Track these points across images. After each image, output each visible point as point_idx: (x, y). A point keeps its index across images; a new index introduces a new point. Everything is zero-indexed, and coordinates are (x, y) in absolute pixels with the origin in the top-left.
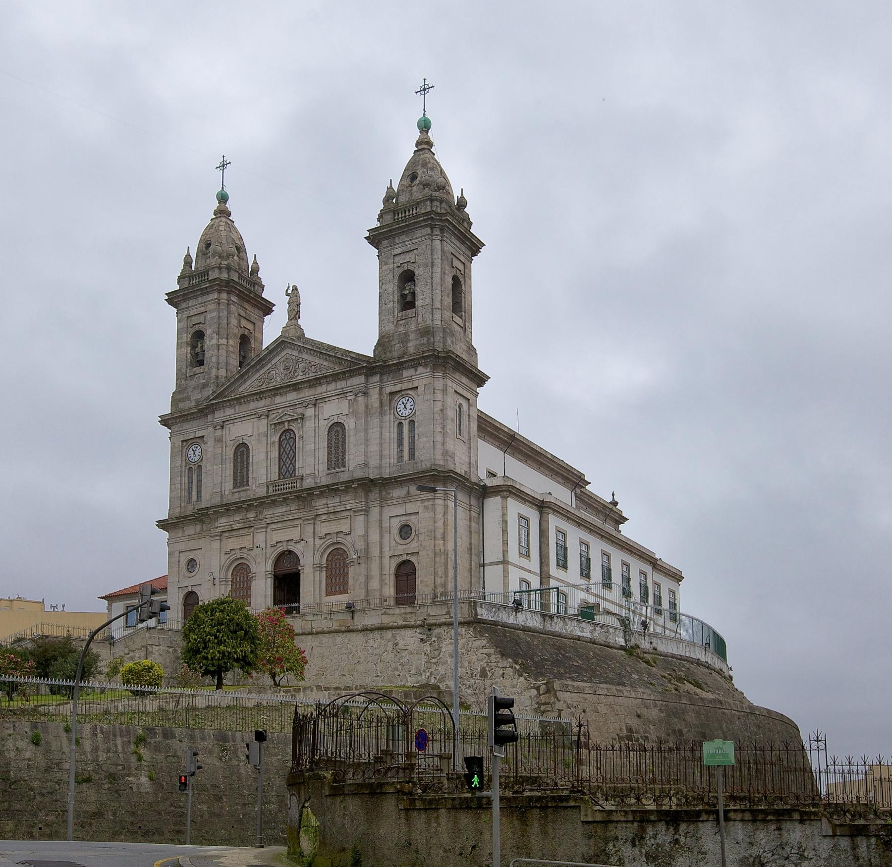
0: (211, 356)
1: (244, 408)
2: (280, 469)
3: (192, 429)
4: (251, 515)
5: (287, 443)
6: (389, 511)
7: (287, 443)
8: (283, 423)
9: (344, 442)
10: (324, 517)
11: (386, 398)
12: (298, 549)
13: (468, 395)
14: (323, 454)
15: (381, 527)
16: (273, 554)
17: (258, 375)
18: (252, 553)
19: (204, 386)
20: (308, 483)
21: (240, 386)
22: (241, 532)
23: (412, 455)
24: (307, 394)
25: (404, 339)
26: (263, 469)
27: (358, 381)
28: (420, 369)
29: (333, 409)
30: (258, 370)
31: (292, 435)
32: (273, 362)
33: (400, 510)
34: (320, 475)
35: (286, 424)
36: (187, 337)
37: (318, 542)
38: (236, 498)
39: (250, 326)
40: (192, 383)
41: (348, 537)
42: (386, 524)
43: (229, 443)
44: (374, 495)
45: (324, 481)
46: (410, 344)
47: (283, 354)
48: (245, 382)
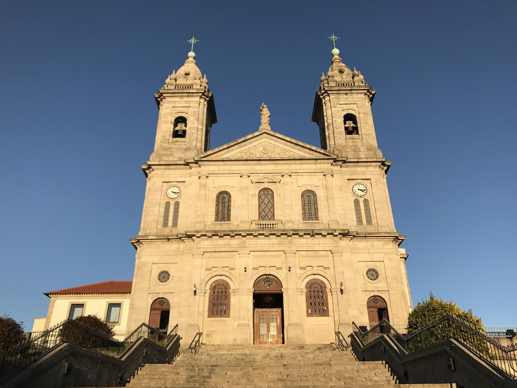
1: (226, 167)
2: (259, 214)
4: (236, 241)
5: (266, 197)
7: (266, 197)
9: (316, 203)
12: (281, 275)
17: (240, 150)
21: (226, 153)
22: (223, 254)
23: (369, 222)
25: (356, 150)
26: (245, 211)
27: (326, 166)
28: (370, 169)
29: (306, 182)
30: (241, 147)
31: (270, 192)
32: (254, 144)
33: (367, 257)
43: (212, 189)
44: (345, 242)
46: (361, 153)
48: (229, 152)
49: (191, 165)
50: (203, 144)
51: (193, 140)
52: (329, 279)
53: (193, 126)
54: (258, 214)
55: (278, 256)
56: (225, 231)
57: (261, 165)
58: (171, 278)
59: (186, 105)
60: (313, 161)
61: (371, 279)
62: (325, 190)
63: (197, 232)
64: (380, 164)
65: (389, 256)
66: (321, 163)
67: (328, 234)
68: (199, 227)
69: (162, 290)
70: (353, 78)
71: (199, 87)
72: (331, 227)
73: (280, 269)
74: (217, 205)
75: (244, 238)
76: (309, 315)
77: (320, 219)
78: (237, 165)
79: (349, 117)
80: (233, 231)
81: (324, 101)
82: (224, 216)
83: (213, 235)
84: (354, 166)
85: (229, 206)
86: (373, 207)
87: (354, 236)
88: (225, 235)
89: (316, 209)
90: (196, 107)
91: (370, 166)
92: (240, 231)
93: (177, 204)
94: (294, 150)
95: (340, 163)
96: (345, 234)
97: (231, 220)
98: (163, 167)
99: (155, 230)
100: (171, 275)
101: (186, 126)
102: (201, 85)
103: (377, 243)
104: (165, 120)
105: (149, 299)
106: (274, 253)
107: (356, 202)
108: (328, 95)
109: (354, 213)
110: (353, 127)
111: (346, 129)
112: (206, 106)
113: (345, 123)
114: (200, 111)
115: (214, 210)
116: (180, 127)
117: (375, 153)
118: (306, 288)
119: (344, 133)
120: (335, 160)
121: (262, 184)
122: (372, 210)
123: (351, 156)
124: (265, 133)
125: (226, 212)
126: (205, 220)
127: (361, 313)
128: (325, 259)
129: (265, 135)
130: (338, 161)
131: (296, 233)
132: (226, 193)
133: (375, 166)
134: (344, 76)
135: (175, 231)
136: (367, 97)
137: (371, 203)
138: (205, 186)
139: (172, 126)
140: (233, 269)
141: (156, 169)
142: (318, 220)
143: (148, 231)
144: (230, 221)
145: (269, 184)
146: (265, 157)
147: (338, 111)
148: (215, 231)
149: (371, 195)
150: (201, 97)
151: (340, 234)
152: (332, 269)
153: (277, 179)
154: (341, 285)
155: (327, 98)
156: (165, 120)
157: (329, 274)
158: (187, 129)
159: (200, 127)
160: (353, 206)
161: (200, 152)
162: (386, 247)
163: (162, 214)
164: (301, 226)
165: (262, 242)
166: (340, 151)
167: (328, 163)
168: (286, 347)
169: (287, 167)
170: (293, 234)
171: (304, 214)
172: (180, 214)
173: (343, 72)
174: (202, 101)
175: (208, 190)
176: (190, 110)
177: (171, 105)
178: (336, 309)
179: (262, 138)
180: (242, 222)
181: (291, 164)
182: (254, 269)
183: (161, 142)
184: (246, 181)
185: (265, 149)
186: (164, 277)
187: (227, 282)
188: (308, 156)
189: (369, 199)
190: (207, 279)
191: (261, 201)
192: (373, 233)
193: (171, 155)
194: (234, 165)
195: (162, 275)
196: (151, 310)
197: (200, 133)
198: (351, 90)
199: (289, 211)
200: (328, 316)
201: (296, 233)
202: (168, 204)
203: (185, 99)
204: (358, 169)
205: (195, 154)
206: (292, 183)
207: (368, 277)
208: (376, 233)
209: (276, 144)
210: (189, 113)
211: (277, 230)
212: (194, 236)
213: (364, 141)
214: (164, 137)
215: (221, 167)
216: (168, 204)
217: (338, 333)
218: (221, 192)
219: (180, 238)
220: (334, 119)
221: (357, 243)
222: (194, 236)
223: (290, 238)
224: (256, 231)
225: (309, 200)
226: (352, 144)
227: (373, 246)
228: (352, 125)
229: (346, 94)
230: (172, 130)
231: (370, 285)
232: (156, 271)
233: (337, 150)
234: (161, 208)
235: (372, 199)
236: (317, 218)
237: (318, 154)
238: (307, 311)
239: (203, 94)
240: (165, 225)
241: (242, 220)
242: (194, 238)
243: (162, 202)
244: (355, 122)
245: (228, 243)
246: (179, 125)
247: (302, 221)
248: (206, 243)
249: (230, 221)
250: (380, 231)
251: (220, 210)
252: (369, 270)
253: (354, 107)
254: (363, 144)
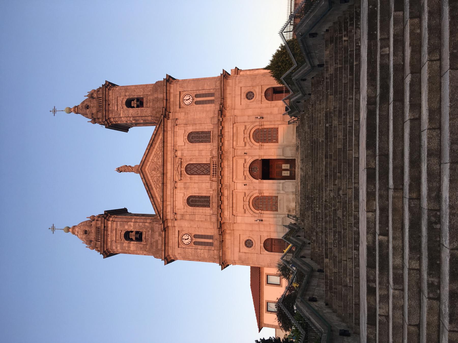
1: (169, 199)
4: (226, 193)
6: (238, 106)
9: (198, 133)
10: (235, 143)
12: (250, 160)
14: (201, 146)
17: (154, 189)
20: (215, 153)
22: (234, 201)
23: (212, 95)
25: (157, 100)
26: (202, 186)
27: (169, 124)
28: (172, 91)
30: (152, 188)
31: (189, 166)
32: (150, 178)
33: (238, 99)
34: (212, 147)
35: (182, 169)
38: (215, 205)
43: (185, 210)
44: (228, 113)
46: (159, 97)
47: (147, 172)
48: (156, 197)
49: (166, 226)
50: (147, 218)
51: (145, 225)
52: (252, 126)
53: (132, 226)
54: (205, 176)
55: (237, 161)
56: (218, 200)
57: (167, 173)
58: (250, 238)
59: (114, 232)
60: (165, 133)
61: (253, 97)
62: (188, 125)
63: (218, 220)
64: (168, 84)
65: (237, 83)
66: (167, 127)
67: (221, 125)
68: (214, 219)
69: (258, 245)
70: (94, 98)
71: (99, 223)
72: (216, 123)
73: (245, 160)
74: (198, 206)
75: (223, 186)
76: (277, 142)
77: (210, 130)
78: (166, 191)
79: (129, 104)
80: (218, 194)
81: (114, 123)
82: (206, 201)
83: (220, 208)
84: (169, 103)
85: (199, 197)
86: (201, 91)
87: (223, 106)
88: (220, 200)
89: (202, 132)
90: (117, 224)
91: (170, 90)
92: (218, 189)
93: (195, 236)
94: (156, 147)
95: (167, 113)
96: (222, 112)
97: (209, 195)
98: (167, 248)
99: (215, 252)
100: (248, 239)
101: (132, 232)
103: (228, 90)
104: (127, 248)
105: (264, 253)
106: (234, 164)
107: (197, 103)
108: (109, 119)
109: (205, 105)
110: (137, 101)
111: (138, 106)
112: (116, 216)
113: (133, 107)
114: (120, 220)
115: (202, 208)
116: (133, 236)
117: (159, 86)
118: (258, 143)
119: (142, 108)
120: (165, 116)
121: (182, 172)
122: (204, 92)
123: (161, 105)
124: (141, 169)
125: (203, 199)
126: (209, 214)
127: (276, 106)
128: (239, 128)
129: (143, 169)
130: (165, 114)
131: (220, 148)
132: (188, 199)
133: (170, 87)
134: (92, 105)
135: (217, 236)
136: (112, 89)
137: (198, 93)
138: (183, 215)
139: (132, 242)
140: (245, 194)
141: (168, 252)
142: (210, 132)
143: (216, 257)
144: (210, 197)
145: (182, 167)
146: (161, 169)
147: (124, 112)
148: (218, 207)
149: (192, 92)
150: (108, 220)
151: (221, 117)
152: (246, 124)
153: (178, 161)
154: (257, 118)
155: (112, 120)
156: (127, 248)
157: (249, 126)
158: (135, 230)
159: (133, 220)
160: (200, 105)
161: (155, 220)
162: (231, 85)
163: (203, 247)
164: (215, 144)
165: (226, 172)
166: (157, 112)
167: (167, 122)
168: (297, 157)
169: (169, 153)
170: (221, 150)
171: (206, 142)
172: (203, 234)
173: (88, 106)
174: (111, 219)
175: (186, 213)
177: (114, 244)
178: (273, 123)
179: (145, 171)
180: (211, 187)
181: (167, 150)
182: (245, 179)
183: (146, 251)
184: (179, 185)
185: (154, 170)
186: (249, 243)
187: (254, 198)
188: (161, 137)
189: (195, 94)
190: (252, 213)
191: (195, 173)
192: (221, 93)
193: (157, 242)
194: (166, 193)
195: (247, 245)
196: (272, 251)
197: (138, 221)
198: (106, 100)
199: (203, 153)
200: (278, 128)
201: (220, 148)
202: (195, 243)
203: (109, 233)
204: (172, 100)
205: (156, 224)
206: (182, 150)
207: (252, 99)
208: (221, 91)
209: (150, 160)
210: (122, 229)
211: (218, 161)
212: (220, 222)
213: (149, 93)
214: (141, 248)
215: (168, 203)
216: (195, 243)
217: (289, 123)
218: (188, 203)
219: (222, 232)
220: (130, 115)
221: (227, 105)
222: (220, 222)
223: (224, 152)
224: (218, 177)
225: (195, 137)
226: (151, 103)
227: (230, 94)
228: (135, 102)
229: (109, 105)
230: (135, 242)
231: (257, 98)
232: (245, 249)
233: (156, 114)
234: (199, 248)
235: (195, 92)
236: (209, 132)
237: (160, 129)
238: (274, 142)
239: (105, 218)
240: (211, 244)
241: (209, 187)
242: (222, 222)
243: (194, 248)
244: (133, 100)
245: (226, 198)
246: (131, 238)
247: (211, 143)
248: (227, 214)
249: (210, 197)
250: (219, 87)
251: (201, 204)
252: (247, 98)
253: (120, 99)
254: (152, 95)
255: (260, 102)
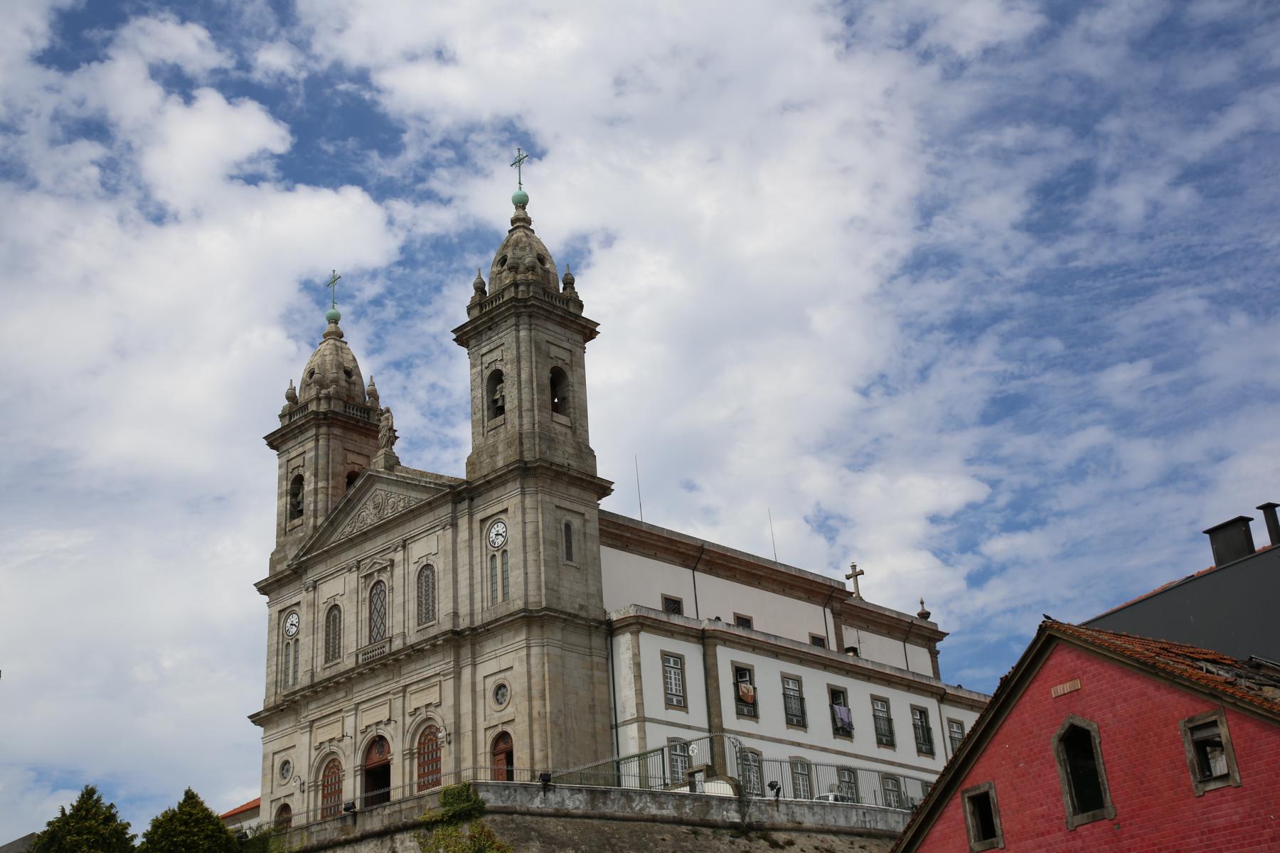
0: (308, 503)
2: (371, 631)
3: (292, 596)
8: (372, 574)
11: (476, 525)
12: (386, 732)
13: (582, 509)
14: (412, 607)
15: (474, 691)
16: (362, 741)
18: (342, 744)
19: (301, 539)
24: (396, 536)
27: (445, 511)
30: (348, 514)
36: (287, 486)
37: (408, 720)
39: (361, 460)
40: (290, 538)
41: (439, 710)
42: (479, 688)
45: (413, 639)
59: (301, 450)
74: (327, 635)
90: (310, 450)
102: (318, 399)
176: (307, 456)
204: (495, 494)
255: (487, 724)
